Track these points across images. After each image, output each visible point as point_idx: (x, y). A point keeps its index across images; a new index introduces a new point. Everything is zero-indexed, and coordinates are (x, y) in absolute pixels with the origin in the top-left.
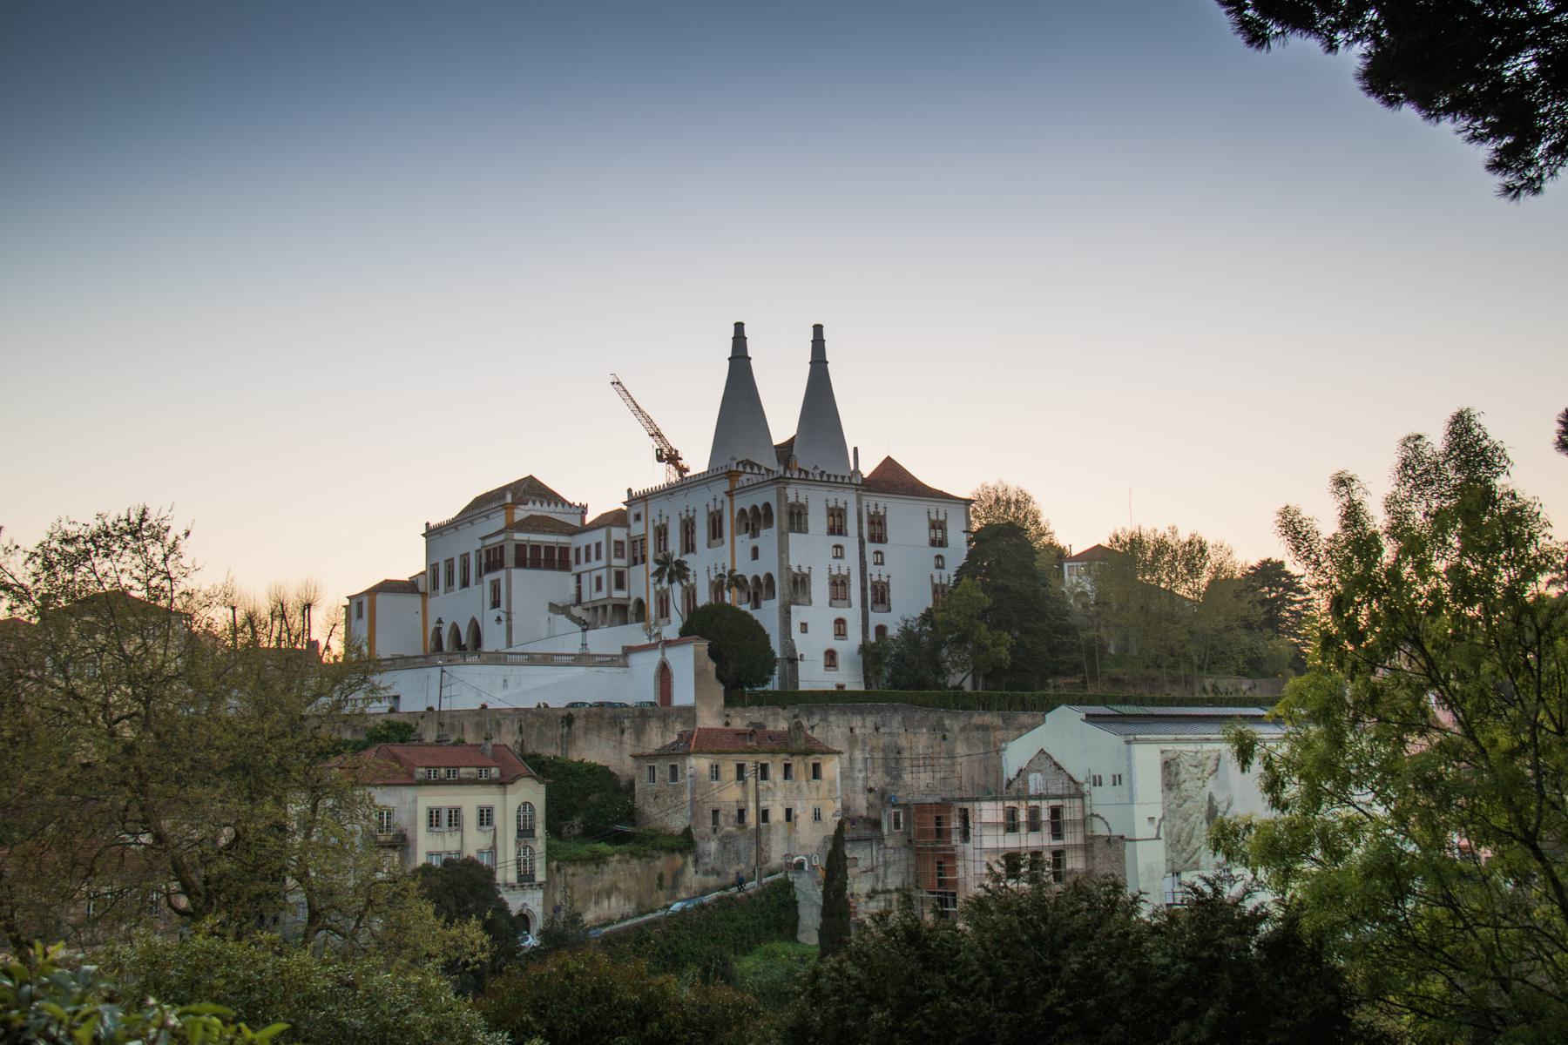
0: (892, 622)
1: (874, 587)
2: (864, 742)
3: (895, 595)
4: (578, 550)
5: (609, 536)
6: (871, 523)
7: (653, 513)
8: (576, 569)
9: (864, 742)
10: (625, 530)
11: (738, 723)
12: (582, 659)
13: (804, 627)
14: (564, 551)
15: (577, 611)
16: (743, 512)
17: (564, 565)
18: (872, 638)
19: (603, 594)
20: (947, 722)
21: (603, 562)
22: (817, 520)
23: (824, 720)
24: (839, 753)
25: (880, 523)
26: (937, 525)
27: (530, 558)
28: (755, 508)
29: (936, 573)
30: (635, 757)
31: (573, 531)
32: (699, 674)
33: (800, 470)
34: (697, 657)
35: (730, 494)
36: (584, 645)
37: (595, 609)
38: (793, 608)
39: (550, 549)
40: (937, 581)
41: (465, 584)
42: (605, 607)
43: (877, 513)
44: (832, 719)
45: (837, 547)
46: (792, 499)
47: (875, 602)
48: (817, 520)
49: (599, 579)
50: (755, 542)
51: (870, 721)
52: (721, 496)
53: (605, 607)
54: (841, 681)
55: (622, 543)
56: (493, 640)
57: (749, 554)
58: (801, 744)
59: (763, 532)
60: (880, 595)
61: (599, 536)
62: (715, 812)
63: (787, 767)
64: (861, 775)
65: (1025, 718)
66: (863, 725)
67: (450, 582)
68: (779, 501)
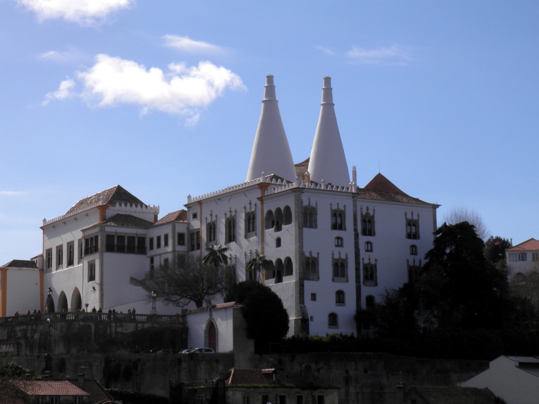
1: (366, 267)
3: (381, 274)
4: (151, 240)
6: (364, 221)
7: (206, 214)
8: (150, 253)
13: (314, 297)
14: (142, 240)
16: (270, 212)
18: (364, 305)
21: (170, 249)
26: (412, 224)
28: (278, 210)
31: (147, 225)
35: (261, 199)
38: (306, 283)
39: (131, 239)
43: (368, 214)
45: (338, 238)
46: (305, 203)
47: (366, 278)
50: (279, 234)
52: (255, 201)
57: (274, 243)
60: (369, 274)
67: (59, 262)
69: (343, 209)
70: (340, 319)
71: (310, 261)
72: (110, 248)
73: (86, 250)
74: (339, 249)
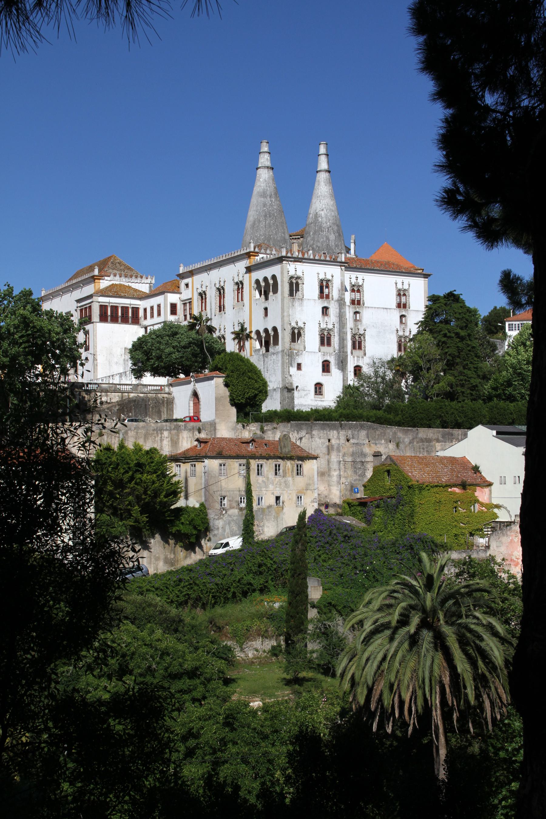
2: (338, 450)
3: (369, 344)
4: (145, 310)
10: (178, 296)
11: (246, 435)
13: (299, 366)
14: (136, 310)
17: (136, 320)
22: (310, 288)
23: (309, 432)
24: (315, 458)
25: (359, 291)
27: (110, 315)
28: (265, 279)
34: (217, 387)
39: (125, 309)
40: (401, 333)
44: (315, 432)
46: (292, 273)
47: (354, 347)
48: (310, 288)
51: (342, 433)
61: (159, 300)
63: (277, 468)
65: (457, 432)
66: (337, 436)
68: (282, 273)
69: (330, 278)
71: (296, 331)
72: (103, 318)
74: (326, 318)
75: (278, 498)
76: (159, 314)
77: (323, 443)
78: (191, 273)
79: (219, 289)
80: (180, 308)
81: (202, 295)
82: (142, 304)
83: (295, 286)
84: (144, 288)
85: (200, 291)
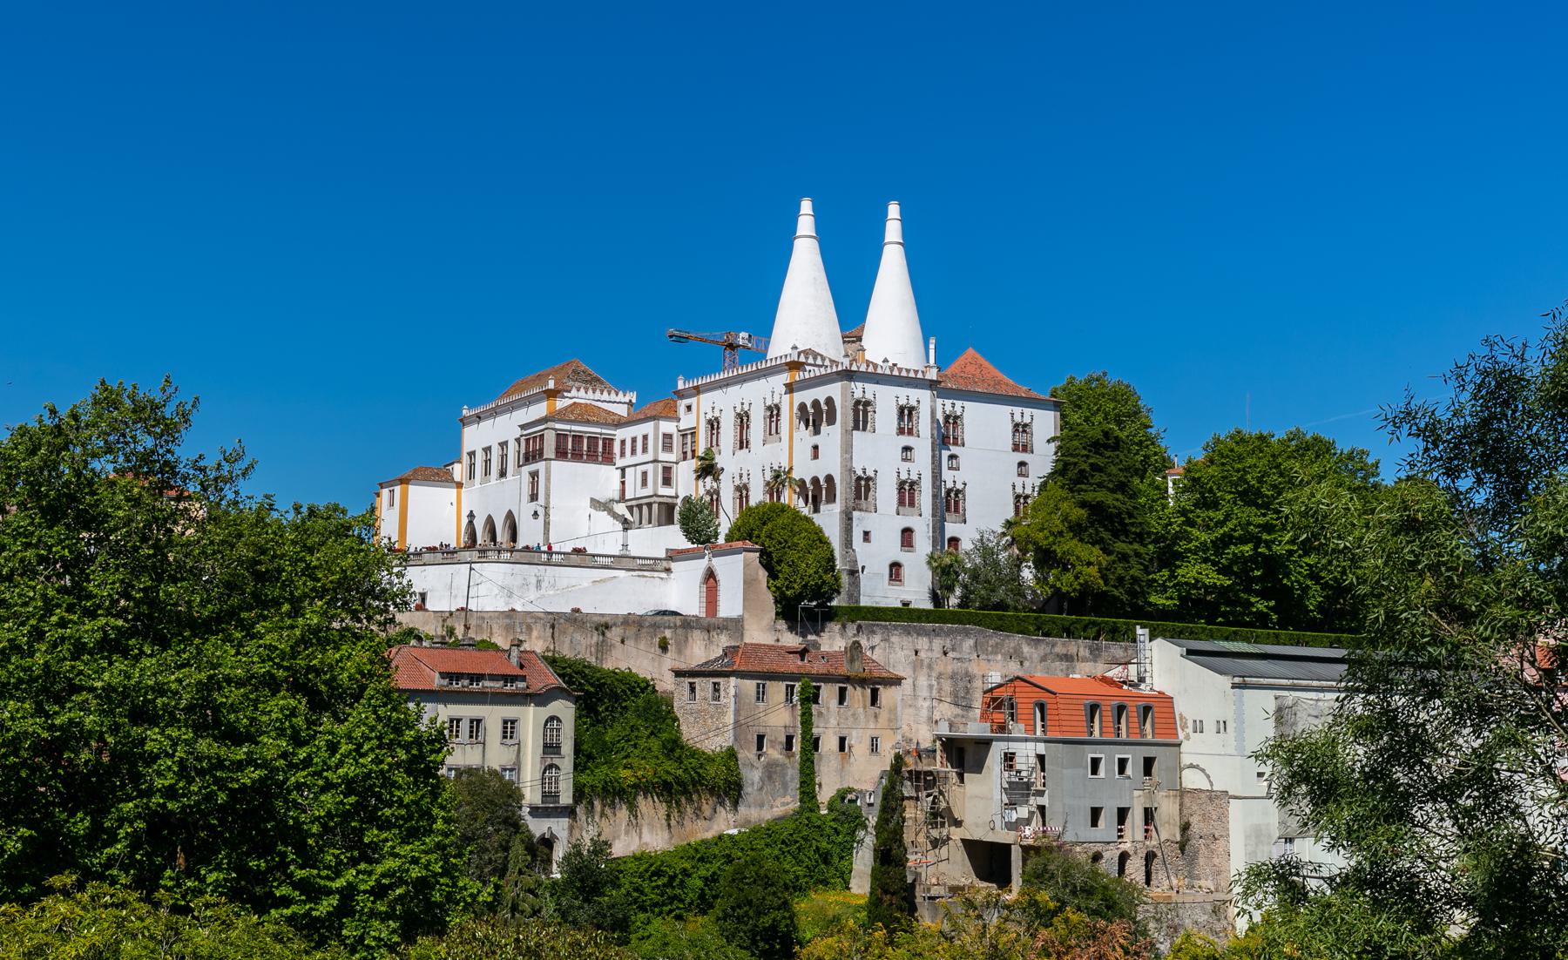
0: (967, 534)
2: (930, 667)
3: (971, 504)
4: (623, 442)
5: (657, 428)
8: (620, 462)
9: (930, 667)
12: (623, 561)
13: (866, 534)
15: (621, 509)
16: (803, 407)
17: (608, 459)
19: (648, 491)
20: (1026, 649)
21: (649, 457)
28: (816, 403)
29: (1019, 481)
30: (679, 674)
32: (749, 583)
33: (868, 363)
34: (746, 566)
36: (625, 546)
37: (640, 507)
38: (856, 514)
39: (593, 440)
40: (1019, 490)
41: (503, 474)
42: (650, 505)
45: (907, 449)
46: (858, 395)
49: (645, 474)
50: (816, 440)
51: (938, 643)
53: (650, 505)
54: (907, 598)
55: (670, 436)
56: (529, 534)
57: (809, 452)
58: (856, 669)
59: (824, 428)
60: (949, 502)
61: (647, 428)
62: (761, 738)
63: (842, 692)
64: (927, 704)
67: (487, 472)
70: (906, 572)
72: (561, 454)
73: (527, 453)
74: (907, 464)
75: (842, 740)
76: (645, 450)
77: (907, 657)
78: (697, 391)
79: (740, 416)
80: (676, 440)
81: (714, 425)
82: (620, 434)
83: (861, 414)
84: (622, 411)
85: (709, 416)
